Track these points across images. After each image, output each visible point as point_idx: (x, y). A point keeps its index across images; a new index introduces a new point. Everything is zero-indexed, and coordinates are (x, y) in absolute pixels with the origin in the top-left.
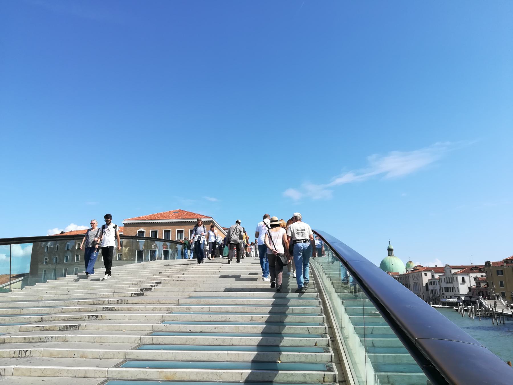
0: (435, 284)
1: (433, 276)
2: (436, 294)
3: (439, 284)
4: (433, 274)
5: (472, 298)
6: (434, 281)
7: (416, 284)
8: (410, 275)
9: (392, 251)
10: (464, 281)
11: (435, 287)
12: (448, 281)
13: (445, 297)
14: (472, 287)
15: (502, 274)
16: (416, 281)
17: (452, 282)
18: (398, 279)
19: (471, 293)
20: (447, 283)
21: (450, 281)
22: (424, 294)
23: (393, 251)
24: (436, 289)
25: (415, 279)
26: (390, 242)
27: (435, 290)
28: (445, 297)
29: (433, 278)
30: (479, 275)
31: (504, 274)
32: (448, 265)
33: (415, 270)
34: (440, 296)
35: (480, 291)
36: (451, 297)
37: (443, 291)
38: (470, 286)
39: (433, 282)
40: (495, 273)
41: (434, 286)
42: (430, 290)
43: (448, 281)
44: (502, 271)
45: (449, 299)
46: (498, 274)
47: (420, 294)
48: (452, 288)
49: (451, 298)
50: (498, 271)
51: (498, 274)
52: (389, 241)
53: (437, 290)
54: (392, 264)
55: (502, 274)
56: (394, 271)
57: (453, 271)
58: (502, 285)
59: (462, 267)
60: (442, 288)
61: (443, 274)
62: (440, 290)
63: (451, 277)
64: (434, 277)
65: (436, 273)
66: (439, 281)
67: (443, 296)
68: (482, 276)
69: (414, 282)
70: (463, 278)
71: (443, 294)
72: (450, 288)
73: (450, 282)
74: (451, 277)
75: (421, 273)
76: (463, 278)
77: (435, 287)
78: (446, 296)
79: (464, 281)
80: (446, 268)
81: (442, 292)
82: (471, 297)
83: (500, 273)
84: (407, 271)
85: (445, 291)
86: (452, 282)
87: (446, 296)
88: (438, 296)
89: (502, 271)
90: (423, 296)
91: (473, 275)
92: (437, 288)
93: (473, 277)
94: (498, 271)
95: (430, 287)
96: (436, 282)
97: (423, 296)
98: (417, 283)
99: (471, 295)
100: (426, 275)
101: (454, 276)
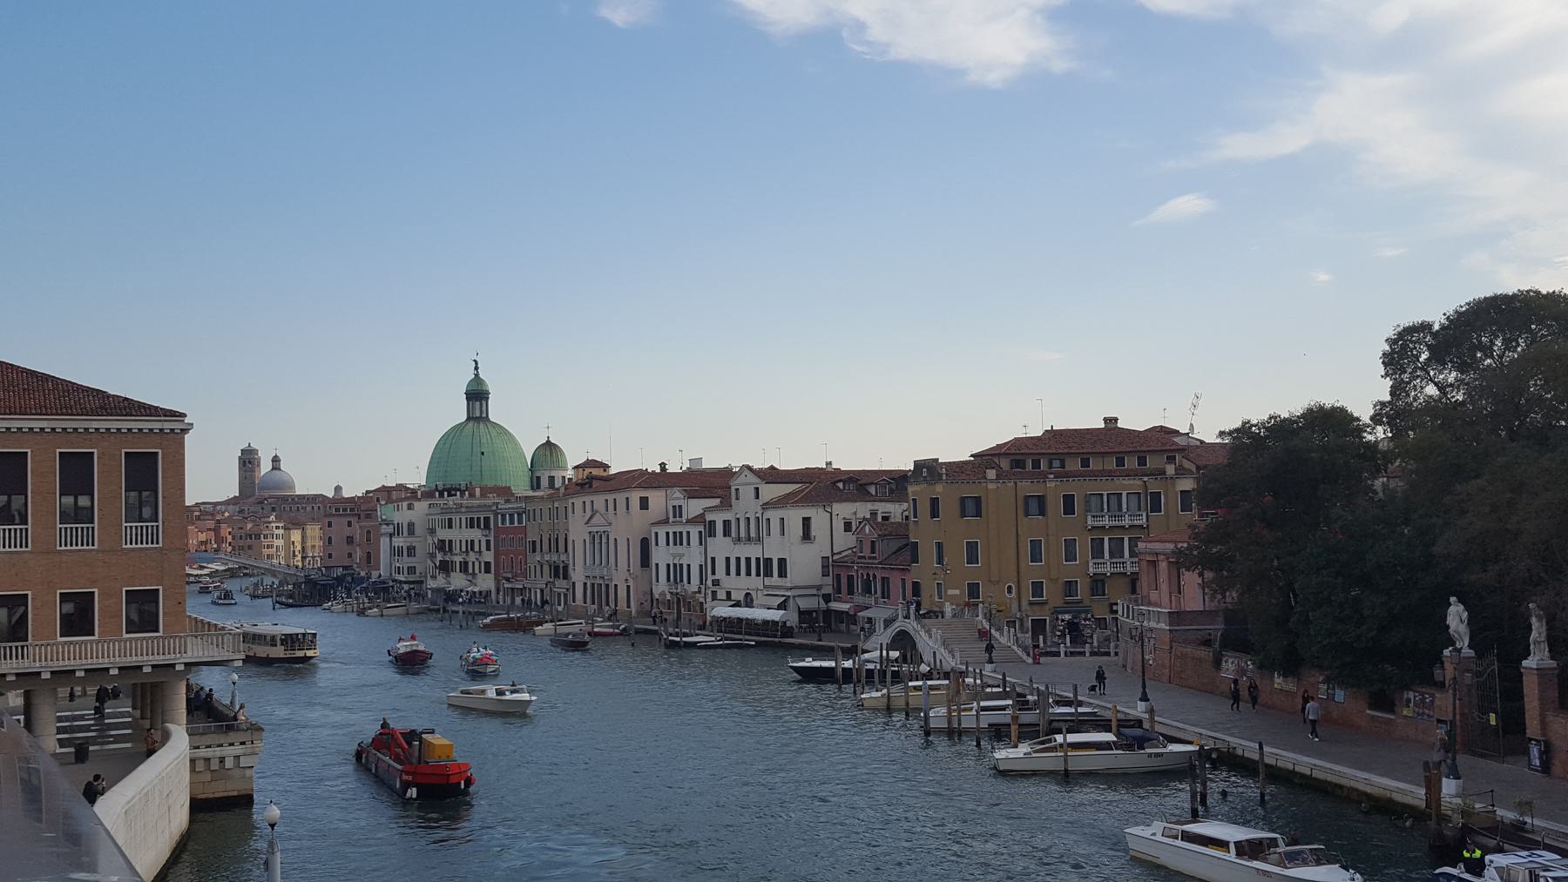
0: (681, 544)
1: (678, 511)
2: (682, 581)
3: (701, 544)
4: (677, 503)
5: (830, 601)
6: (678, 529)
7: (597, 541)
8: (573, 503)
9: (484, 403)
10: (807, 536)
11: (681, 556)
12: (743, 534)
13: (722, 595)
14: (835, 557)
15: (978, 514)
16: (602, 529)
17: (759, 539)
18: (520, 515)
19: (829, 580)
20: (739, 539)
21: (753, 535)
22: (631, 583)
23: (488, 398)
24: (685, 562)
25: (597, 519)
26: (479, 366)
27: (681, 565)
28: (722, 595)
29: (675, 517)
30: (862, 509)
31: (984, 513)
32: (749, 468)
33: (594, 482)
34: (699, 592)
35: (875, 576)
36: (747, 594)
37: (713, 573)
38: (829, 554)
39: (675, 533)
40: (949, 508)
41: (679, 549)
42: (657, 565)
43: (743, 534)
44: (978, 500)
45: (737, 604)
46: (963, 515)
47: (611, 580)
48: (758, 560)
49: (748, 601)
50: (963, 500)
51: (963, 515)
52: (475, 361)
53: (689, 566)
54: (483, 453)
55: (978, 514)
56: (490, 484)
57: (771, 492)
58: (972, 559)
59: (798, 479)
60: (713, 559)
61: (717, 502)
62: (701, 566)
63: (759, 515)
64: (681, 516)
65: (692, 495)
66: (700, 532)
67: (714, 593)
68: (874, 514)
69: (590, 529)
70: (806, 522)
71: (716, 583)
72: (748, 560)
73: (749, 539)
74: (759, 515)
75: (627, 495)
76: (806, 522)
77: (681, 556)
78: (729, 594)
79: (807, 536)
80: (741, 479)
81: (710, 578)
82: (827, 598)
83: (970, 506)
84: (535, 484)
85: (728, 573)
86: (759, 539)
87: (729, 594)
88: (696, 592)
89: (978, 500)
90: (628, 587)
91: (843, 510)
92: (693, 557)
93: (841, 517)
94: (963, 500)
95: (661, 555)
96: (688, 533)
97: (628, 587)
98: (601, 536)
99: (828, 590)
100: (644, 503)
101: (770, 514)
